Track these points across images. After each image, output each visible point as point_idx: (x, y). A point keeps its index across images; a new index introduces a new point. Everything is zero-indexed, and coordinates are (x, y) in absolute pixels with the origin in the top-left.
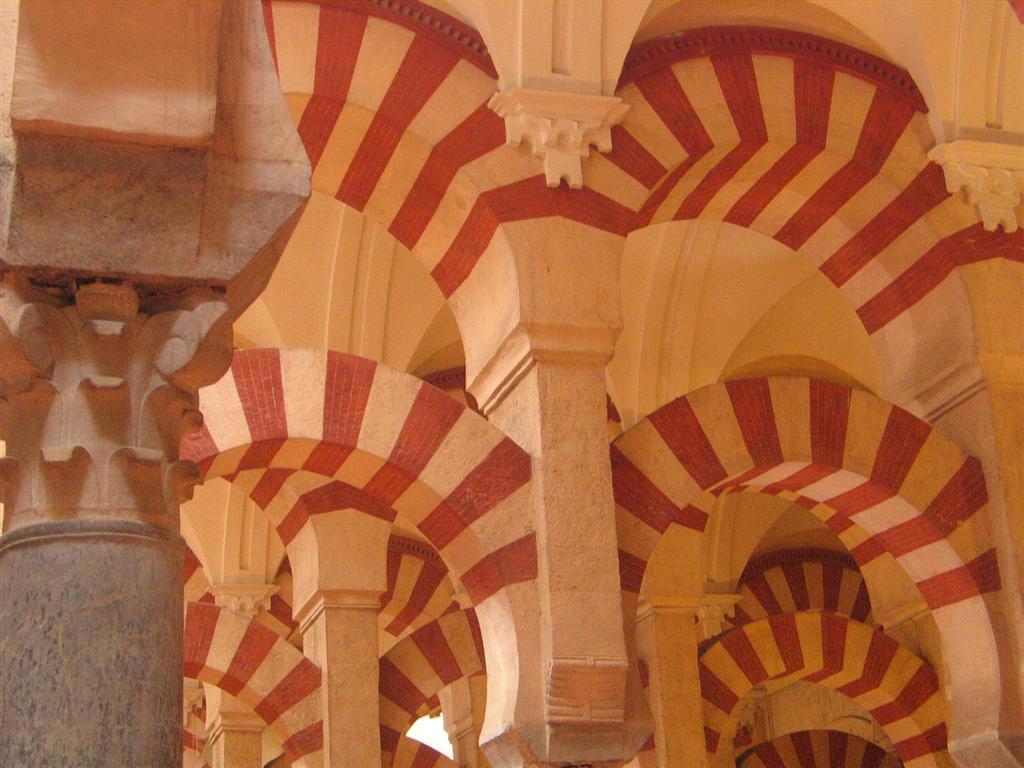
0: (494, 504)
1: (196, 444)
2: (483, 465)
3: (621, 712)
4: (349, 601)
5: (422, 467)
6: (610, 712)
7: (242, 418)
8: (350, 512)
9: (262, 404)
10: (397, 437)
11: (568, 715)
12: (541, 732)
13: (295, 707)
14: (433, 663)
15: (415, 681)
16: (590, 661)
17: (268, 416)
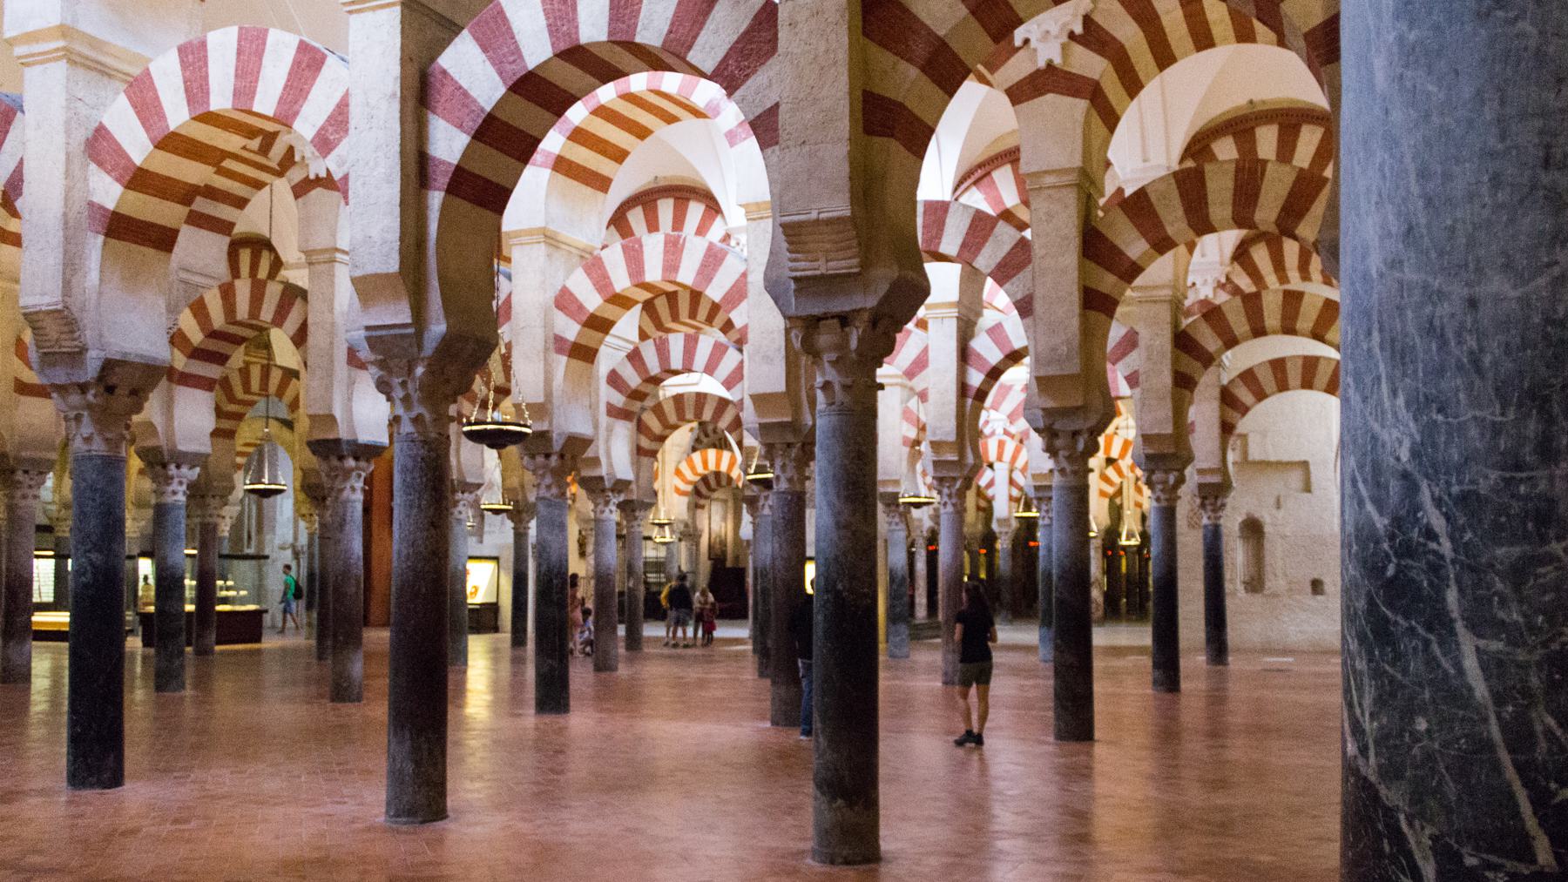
0: (755, 71)
1: (514, 67)
2: (746, 33)
3: (855, 261)
4: (1050, 180)
5: (690, 48)
6: (843, 263)
7: (546, 35)
8: (1050, 97)
9: (561, 18)
10: (669, 22)
11: (807, 268)
12: (787, 289)
13: (1014, 279)
14: (1138, 226)
15: (1118, 242)
16: (814, 215)
17: (565, 28)
